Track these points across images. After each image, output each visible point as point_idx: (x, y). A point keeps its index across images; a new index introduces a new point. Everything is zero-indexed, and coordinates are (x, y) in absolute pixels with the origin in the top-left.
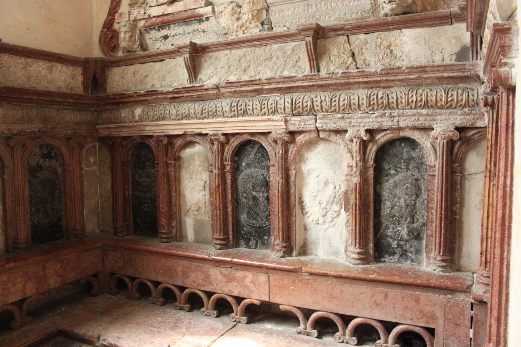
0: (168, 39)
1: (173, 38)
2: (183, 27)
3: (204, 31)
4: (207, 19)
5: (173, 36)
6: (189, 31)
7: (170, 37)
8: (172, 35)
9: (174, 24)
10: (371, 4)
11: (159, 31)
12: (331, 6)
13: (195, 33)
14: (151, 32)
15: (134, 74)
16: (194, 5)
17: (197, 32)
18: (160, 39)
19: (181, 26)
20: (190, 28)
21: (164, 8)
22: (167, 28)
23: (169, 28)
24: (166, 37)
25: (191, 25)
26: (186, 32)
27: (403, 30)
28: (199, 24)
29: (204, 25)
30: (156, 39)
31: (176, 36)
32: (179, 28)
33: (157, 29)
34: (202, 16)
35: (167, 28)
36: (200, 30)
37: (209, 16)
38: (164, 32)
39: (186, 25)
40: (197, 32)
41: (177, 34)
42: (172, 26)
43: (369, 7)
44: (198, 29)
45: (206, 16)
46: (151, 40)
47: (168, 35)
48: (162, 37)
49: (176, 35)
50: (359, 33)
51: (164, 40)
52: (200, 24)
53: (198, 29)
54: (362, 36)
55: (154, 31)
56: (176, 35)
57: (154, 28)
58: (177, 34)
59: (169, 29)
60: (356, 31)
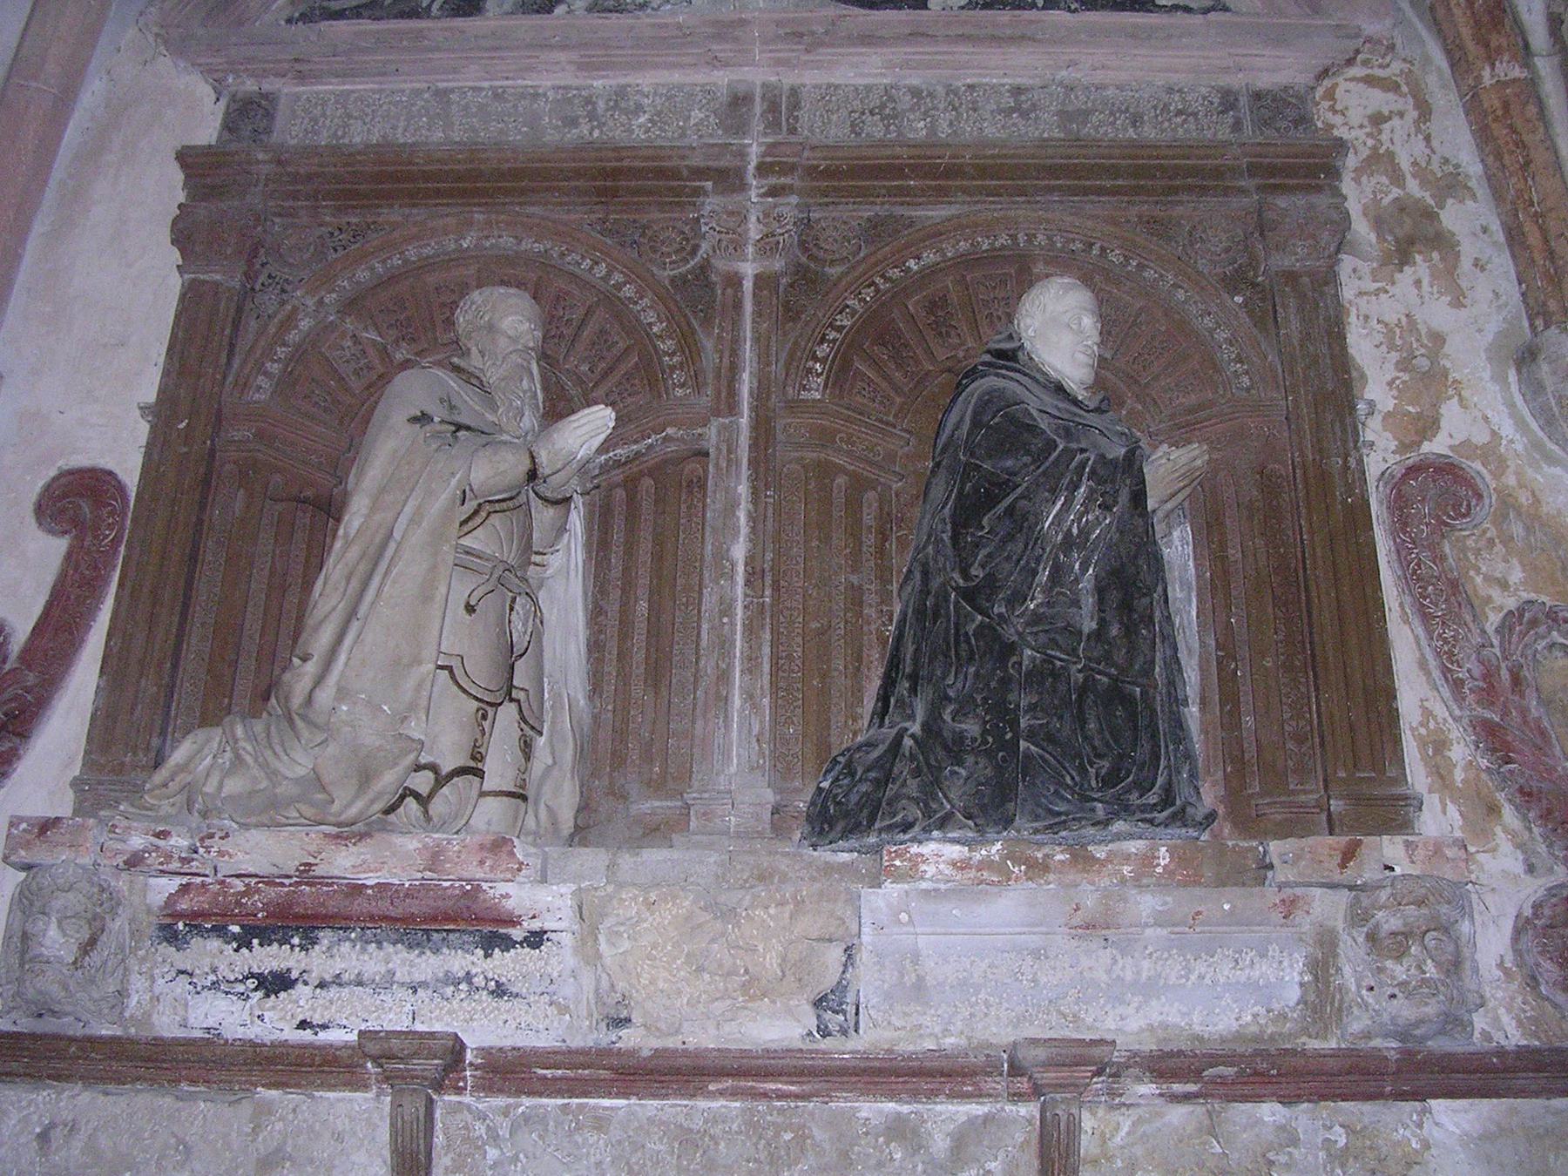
0: (282, 995)
1: (318, 990)
2: (391, 949)
3: (500, 991)
4: (536, 939)
5: (322, 985)
6: (418, 977)
7: (300, 986)
8: (314, 978)
9: (345, 929)
10: (1301, 985)
11: (244, 942)
12: (1138, 973)
13: (449, 990)
14: (196, 942)
15: (44, 1137)
16: (482, 863)
17: (463, 986)
18: (240, 988)
19: (379, 944)
20: (427, 965)
21: (313, 848)
22: (296, 941)
23: (309, 942)
24: (276, 983)
25: (436, 951)
26: (398, 976)
27: (1433, 1103)
28: (480, 952)
29: (502, 964)
30: (215, 985)
31: (333, 991)
32: (364, 950)
33: (235, 937)
34: (513, 922)
35: (296, 941)
36: (479, 981)
37: (547, 926)
38: (268, 958)
39: (410, 947)
40: (463, 986)
41: (345, 977)
42: (326, 937)
43: (1294, 994)
44: (468, 977)
45: (536, 925)
46: (184, 979)
47: (295, 974)
48: (252, 975)
49: (340, 985)
50: (1258, 1098)
51: (260, 994)
52: (487, 956)
53: (468, 977)
54: (1270, 1112)
55: (214, 944)
56: (337, 981)
57: (220, 931)
58: (345, 977)
59: (302, 948)
60: (1246, 1090)
